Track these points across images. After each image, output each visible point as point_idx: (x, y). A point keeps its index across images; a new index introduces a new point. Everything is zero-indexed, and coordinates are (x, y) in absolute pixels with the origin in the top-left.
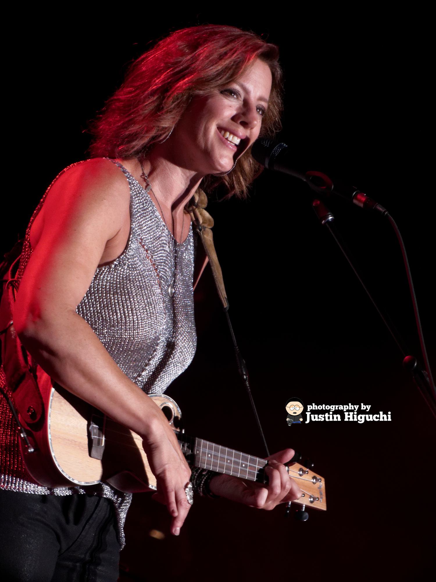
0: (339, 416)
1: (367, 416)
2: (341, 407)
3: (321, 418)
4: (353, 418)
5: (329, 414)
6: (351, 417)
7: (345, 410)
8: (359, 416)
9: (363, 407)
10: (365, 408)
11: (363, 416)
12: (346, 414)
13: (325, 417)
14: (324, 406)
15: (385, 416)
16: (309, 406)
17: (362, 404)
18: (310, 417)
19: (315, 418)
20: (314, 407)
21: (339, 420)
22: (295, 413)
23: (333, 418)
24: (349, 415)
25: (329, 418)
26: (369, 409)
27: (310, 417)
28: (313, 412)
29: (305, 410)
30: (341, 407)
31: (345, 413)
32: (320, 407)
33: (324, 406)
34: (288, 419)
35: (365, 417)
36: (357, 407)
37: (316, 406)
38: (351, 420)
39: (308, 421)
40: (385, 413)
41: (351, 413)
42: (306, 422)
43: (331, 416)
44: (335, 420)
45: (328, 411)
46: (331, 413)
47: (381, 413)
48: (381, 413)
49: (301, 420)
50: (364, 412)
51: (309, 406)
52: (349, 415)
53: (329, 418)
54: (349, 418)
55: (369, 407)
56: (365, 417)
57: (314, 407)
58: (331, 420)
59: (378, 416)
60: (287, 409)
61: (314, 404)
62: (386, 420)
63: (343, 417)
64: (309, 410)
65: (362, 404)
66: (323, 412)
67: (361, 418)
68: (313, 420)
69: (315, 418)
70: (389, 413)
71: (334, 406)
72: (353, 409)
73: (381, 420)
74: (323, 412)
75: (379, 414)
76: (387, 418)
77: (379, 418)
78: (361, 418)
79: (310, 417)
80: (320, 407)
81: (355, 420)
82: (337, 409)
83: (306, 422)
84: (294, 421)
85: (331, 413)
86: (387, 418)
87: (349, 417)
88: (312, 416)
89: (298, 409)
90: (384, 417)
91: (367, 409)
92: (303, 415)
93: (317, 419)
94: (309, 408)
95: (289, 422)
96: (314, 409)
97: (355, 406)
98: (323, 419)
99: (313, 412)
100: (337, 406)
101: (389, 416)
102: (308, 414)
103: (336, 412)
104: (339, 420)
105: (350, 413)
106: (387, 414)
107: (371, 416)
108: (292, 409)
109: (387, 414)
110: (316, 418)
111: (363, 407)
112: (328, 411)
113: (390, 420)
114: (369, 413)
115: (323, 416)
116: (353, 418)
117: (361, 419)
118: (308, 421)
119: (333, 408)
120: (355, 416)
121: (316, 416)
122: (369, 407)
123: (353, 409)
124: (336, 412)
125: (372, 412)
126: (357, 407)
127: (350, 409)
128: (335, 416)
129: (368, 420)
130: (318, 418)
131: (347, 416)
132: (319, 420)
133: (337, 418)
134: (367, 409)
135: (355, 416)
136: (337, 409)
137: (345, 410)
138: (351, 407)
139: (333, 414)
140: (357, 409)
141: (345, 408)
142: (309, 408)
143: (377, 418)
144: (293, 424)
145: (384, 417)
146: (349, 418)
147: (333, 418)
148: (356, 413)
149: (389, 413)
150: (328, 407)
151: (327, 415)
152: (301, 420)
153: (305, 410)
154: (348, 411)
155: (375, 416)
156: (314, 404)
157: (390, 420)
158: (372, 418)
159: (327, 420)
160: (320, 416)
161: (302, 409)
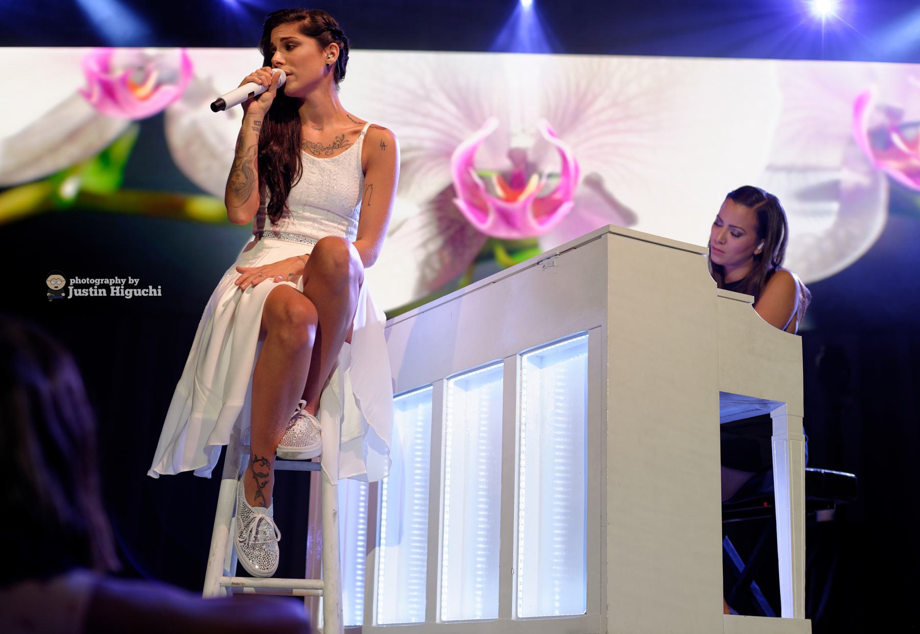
0: (104, 290)
1: (135, 290)
2: (107, 281)
3: (84, 293)
6: (118, 291)
9: (131, 281)
11: (131, 291)
12: (112, 288)
15: (155, 290)
21: (105, 294)
28: (76, 286)
29: (68, 284)
30: (107, 281)
32: (84, 281)
36: (124, 281)
38: (118, 294)
39: (70, 297)
40: (155, 287)
41: (118, 288)
44: (100, 294)
45: (93, 285)
47: (150, 287)
48: (150, 287)
49: (63, 295)
50: (132, 286)
55: (137, 281)
57: (77, 281)
58: (96, 294)
62: (155, 294)
63: (109, 292)
66: (87, 286)
68: (76, 294)
73: (151, 294)
79: (74, 293)
80: (84, 281)
81: (122, 294)
87: (115, 292)
88: (75, 290)
90: (154, 292)
92: (66, 289)
93: (80, 294)
94: (72, 281)
98: (87, 294)
99: (76, 286)
101: (159, 291)
102: (71, 288)
103: (101, 286)
104: (105, 294)
107: (139, 290)
110: (79, 293)
111: (131, 281)
112: (93, 285)
113: (160, 294)
114: (137, 287)
117: (129, 294)
118: (70, 297)
119: (98, 282)
121: (80, 290)
122: (137, 281)
124: (101, 286)
125: (141, 286)
126: (124, 281)
128: (100, 290)
129: (136, 294)
131: (113, 291)
133: (103, 292)
138: (117, 280)
142: (72, 281)
145: (154, 292)
150: (92, 281)
151: (91, 289)
152: (63, 295)
153: (68, 284)
154: (114, 285)
157: (160, 294)
159: (91, 295)
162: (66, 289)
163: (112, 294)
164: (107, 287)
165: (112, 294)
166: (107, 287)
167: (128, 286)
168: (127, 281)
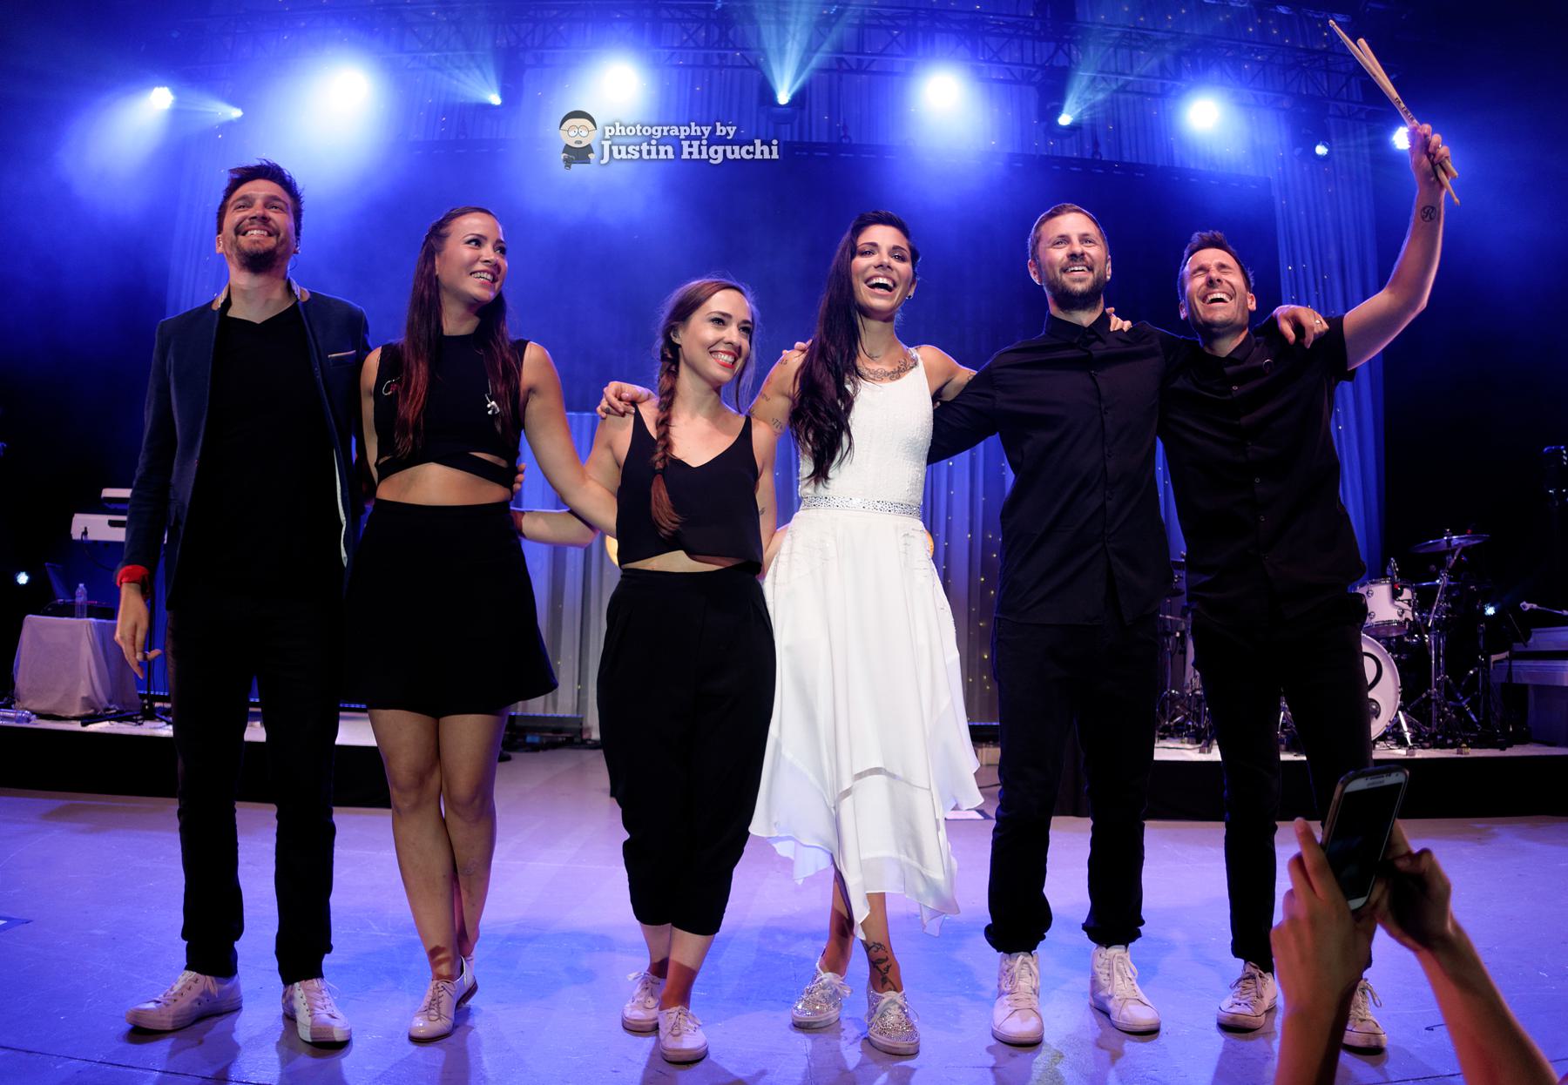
0: (670, 149)
1: (729, 148)
2: (675, 131)
6: (695, 150)
8: (712, 149)
11: (720, 149)
12: (685, 144)
15: (766, 148)
25: (649, 152)
38: (696, 156)
41: (696, 143)
43: (653, 149)
44: (662, 156)
47: (758, 142)
48: (758, 142)
50: (723, 141)
53: (649, 152)
55: (732, 131)
58: (654, 156)
60: (563, 134)
62: (767, 156)
63: (678, 151)
64: (607, 135)
68: (616, 156)
73: (758, 156)
81: (704, 156)
89: (584, 133)
90: (761, 151)
93: (623, 155)
101: (775, 149)
104: (671, 156)
106: (770, 145)
107: (736, 148)
109: (770, 145)
111: (721, 130)
113: (775, 156)
117: (717, 155)
120: (704, 149)
125: (739, 141)
126: (707, 130)
128: (662, 149)
129: (730, 156)
131: (686, 150)
135: (704, 149)
138: (695, 130)
155: (745, 149)
157: (775, 156)
159: (645, 156)
160: (630, 149)
163: (685, 156)
165: (685, 156)
167: (714, 140)
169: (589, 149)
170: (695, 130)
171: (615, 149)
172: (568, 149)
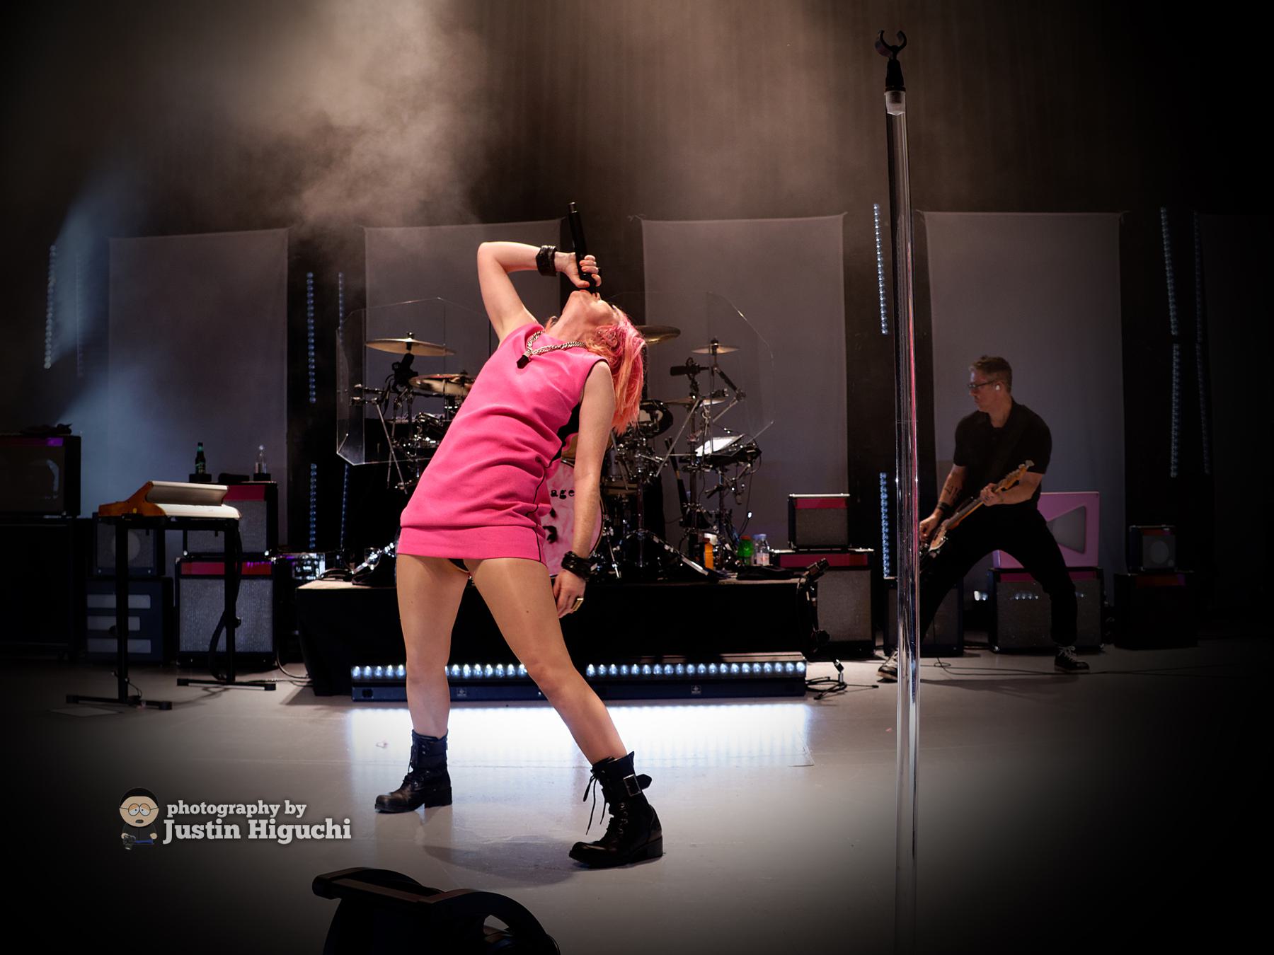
0: (236, 828)
1: (298, 828)
2: (241, 809)
3: (197, 832)
4: (268, 832)
5: (214, 823)
6: (263, 829)
7: (249, 815)
8: (281, 828)
10: (293, 811)
11: (290, 828)
12: (252, 823)
13: (205, 831)
14: (203, 805)
15: (337, 828)
16: (170, 807)
17: (287, 802)
18: (174, 831)
19: (183, 832)
20: (182, 808)
21: (237, 836)
22: (141, 821)
23: (223, 832)
24: (258, 825)
25: (214, 832)
26: (301, 812)
27: (174, 831)
28: (179, 819)
29: (163, 814)
30: (241, 809)
31: (250, 821)
32: (195, 809)
33: (203, 805)
34: (123, 835)
35: (294, 831)
36: (275, 809)
37: (186, 806)
38: (263, 836)
39: (168, 840)
41: (263, 823)
42: (165, 842)
43: (219, 828)
44: (228, 836)
45: (213, 818)
46: (219, 821)
47: (329, 821)
48: (329, 821)
50: (292, 820)
51: (170, 807)
52: (258, 825)
53: (214, 832)
54: (258, 833)
55: (301, 809)
56: (294, 831)
57: (182, 808)
58: (219, 836)
59: (322, 828)
60: (123, 813)
61: (181, 802)
62: (338, 836)
63: (245, 830)
64: (170, 815)
65: (287, 802)
66: (201, 819)
67: (285, 832)
68: (179, 836)
69: (183, 832)
70: (347, 821)
71: (225, 807)
72: (267, 812)
73: (329, 836)
74: (201, 819)
75: (325, 824)
76: (343, 833)
77: (325, 833)
78: (285, 832)
79: (174, 832)
81: (272, 836)
82: (231, 812)
83: (165, 842)
84: (138, 838)
85: (219, 821)
86: (343, 833)
88: (178, 828)
89: (146, 812)
91: (297, 812)
92: (159, 826)
93: (187, 835)
94: (172, 810)
95: (127, 840)
96: (181, 812)
97: (272, 807)
98: (201, 836)
100: (232, 807)
101: (347, 828)
102: (169, 823)
103: (228, 820)
104: (237, 836)
105: (261, 821)
106: (342, 825)
107: (306, 828)
108: (133, 812)
109: (342, 825)
111: (290, 809)
113: (347, 836)
114: (301, 822)
115: (202, 827)
116: (268, 832)
118: (168, 840)
119: (223, 810)
120: (272, 828)
121: (187, 828)
122: (301, 809)
123: (267, 812)
124: (228, 820)
126: (275, 809)
127: (261, 812)
128: (228, 828)
129: (299, 836)
130: (191, 832)
131: (253, 829)
132: (194, 836)
134: (297, 812)
135: (272, 828)
136: (231, 812)
137: (249, 815)
138: (262, 808)
139: (223, 825)
140: (275, 812)
141: (251, 810)
142: (172, 810)
143: (319, 832)
144: (135, 847)
146: (258, 833)
147: (223, 832)
148: (272, 821)
149: (347, 821)
150: (212, 809)
151: (210, 826)
152: (154, 836)
153: (163, 814)
156: (181, 802)
157: (347, 836)
158: (308, 832)
159: (210, 836)
160: (195, 828)
161: (155, 812)
162: (159, 826)
163: (252, 836)
164: (242, 821)
165: (252, 836)
166: (242, 821)
167: (282, 819)
168: (283, 808)
169: (149, 829)
170: (262, 808)
171: (178, 828)
172: (131, 829)
